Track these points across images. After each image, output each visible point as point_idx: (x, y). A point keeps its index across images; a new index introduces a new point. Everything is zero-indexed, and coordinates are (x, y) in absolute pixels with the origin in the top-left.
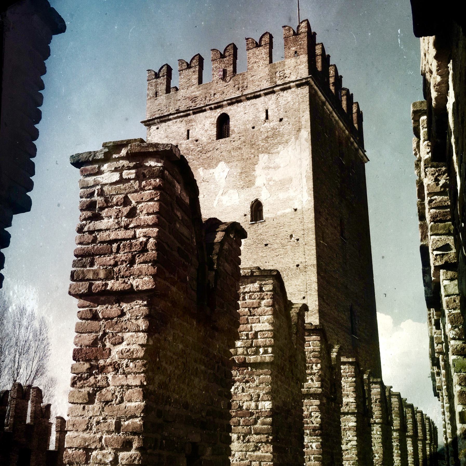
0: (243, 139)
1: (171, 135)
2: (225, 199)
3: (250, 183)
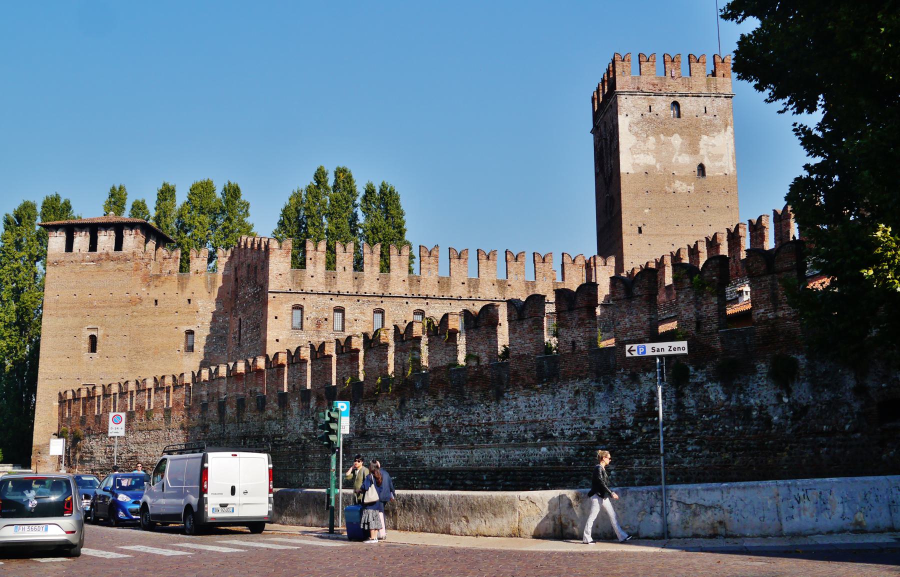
0: (690, 122)
1: (637, 106)
2: (680, 159)
3: (695, 151)
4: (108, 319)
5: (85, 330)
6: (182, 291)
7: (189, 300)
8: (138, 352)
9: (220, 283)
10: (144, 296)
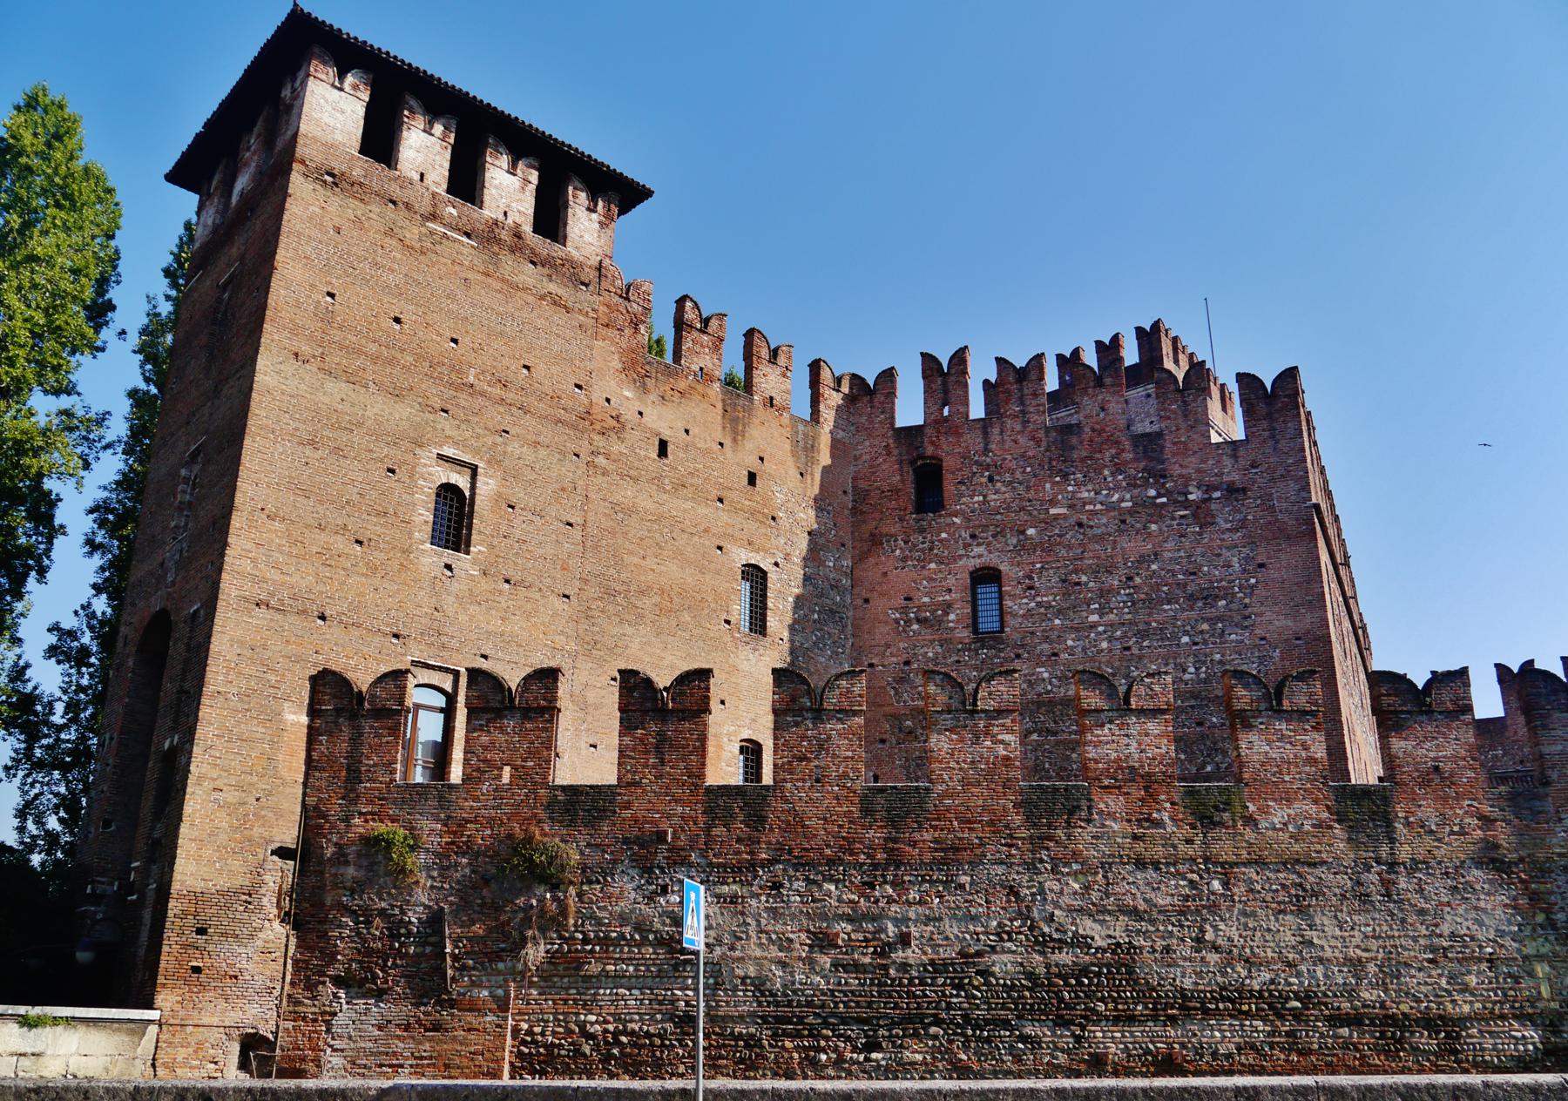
4: (514, 448)
5: (427, 457)
6: (735, 440)
7: (752, 479)
8: (611, 593)
9: (825, 458)
10: (629, 415)
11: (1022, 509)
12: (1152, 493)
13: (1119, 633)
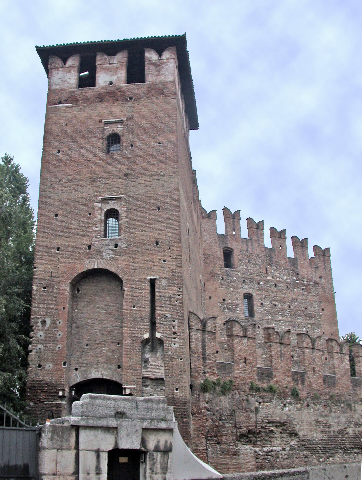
11: (259, 275)
12: (295, 278)
13: (287, 324)
